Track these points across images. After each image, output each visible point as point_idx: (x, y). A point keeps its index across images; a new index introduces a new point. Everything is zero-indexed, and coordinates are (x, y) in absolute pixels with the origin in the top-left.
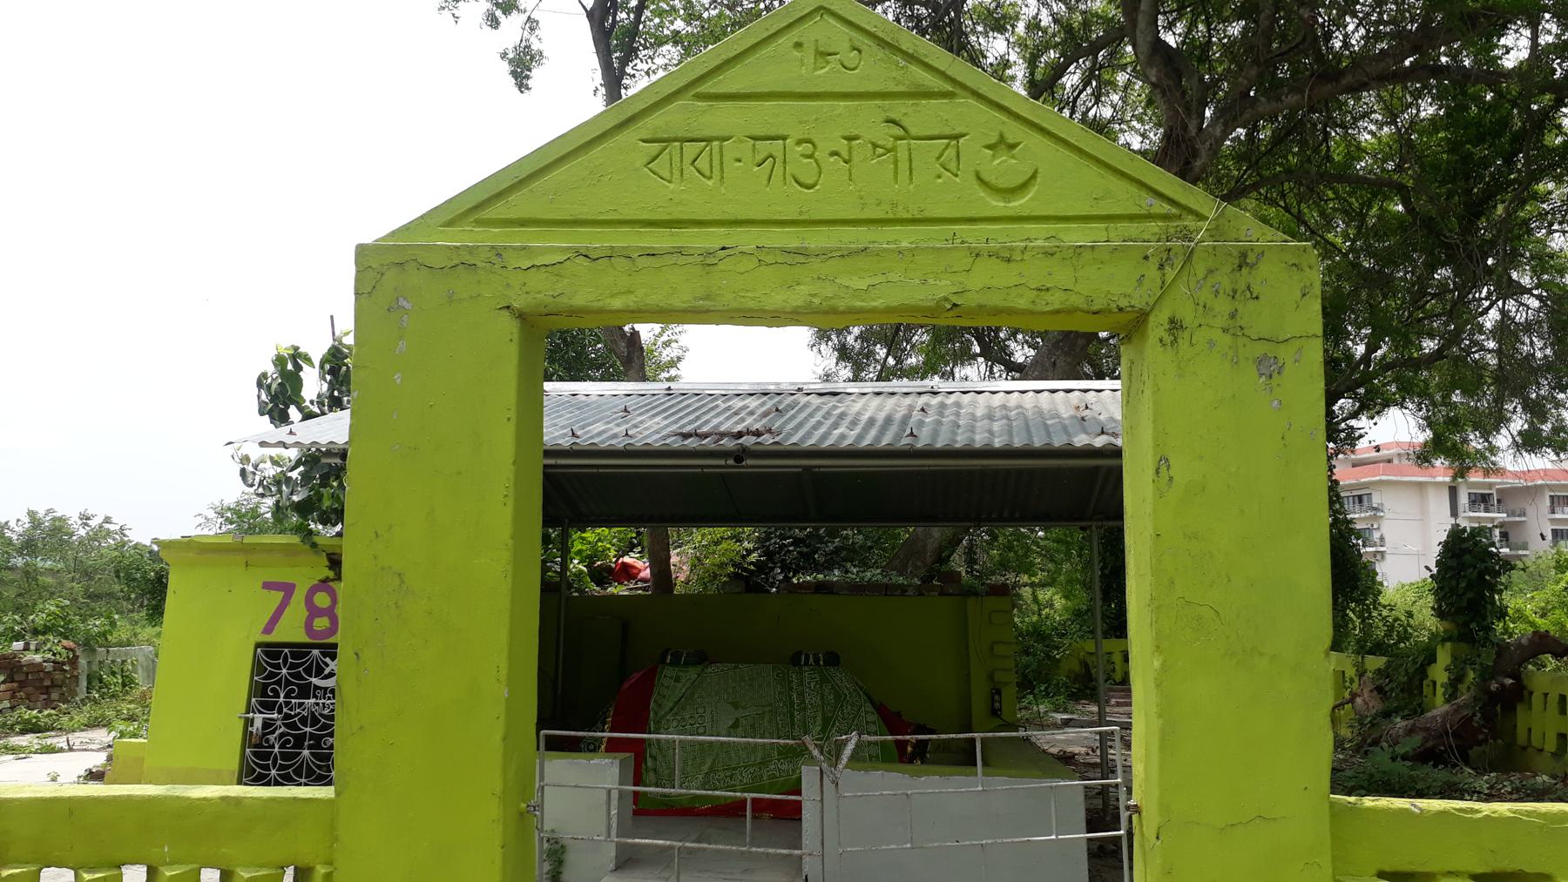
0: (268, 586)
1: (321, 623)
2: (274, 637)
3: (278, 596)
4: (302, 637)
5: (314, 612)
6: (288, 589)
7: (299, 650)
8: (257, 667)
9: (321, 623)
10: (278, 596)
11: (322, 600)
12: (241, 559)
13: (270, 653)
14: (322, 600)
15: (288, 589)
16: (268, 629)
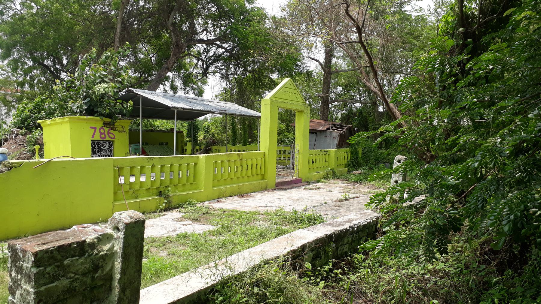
0: (91, 128)
1: (103, 136)
2: (94, 139)
3: (93, 130)
4: (100, 139)
5: (101, 134)
6: (95, 128)
7: (99, 141)
8: (92, 146)
9: (103, 136)
10: (93, 130)
11: (102, 131)
12: (86, 121)
13: (93, 142)
14: (102, 131)
15: (95, 128)
16: (93, 137)
